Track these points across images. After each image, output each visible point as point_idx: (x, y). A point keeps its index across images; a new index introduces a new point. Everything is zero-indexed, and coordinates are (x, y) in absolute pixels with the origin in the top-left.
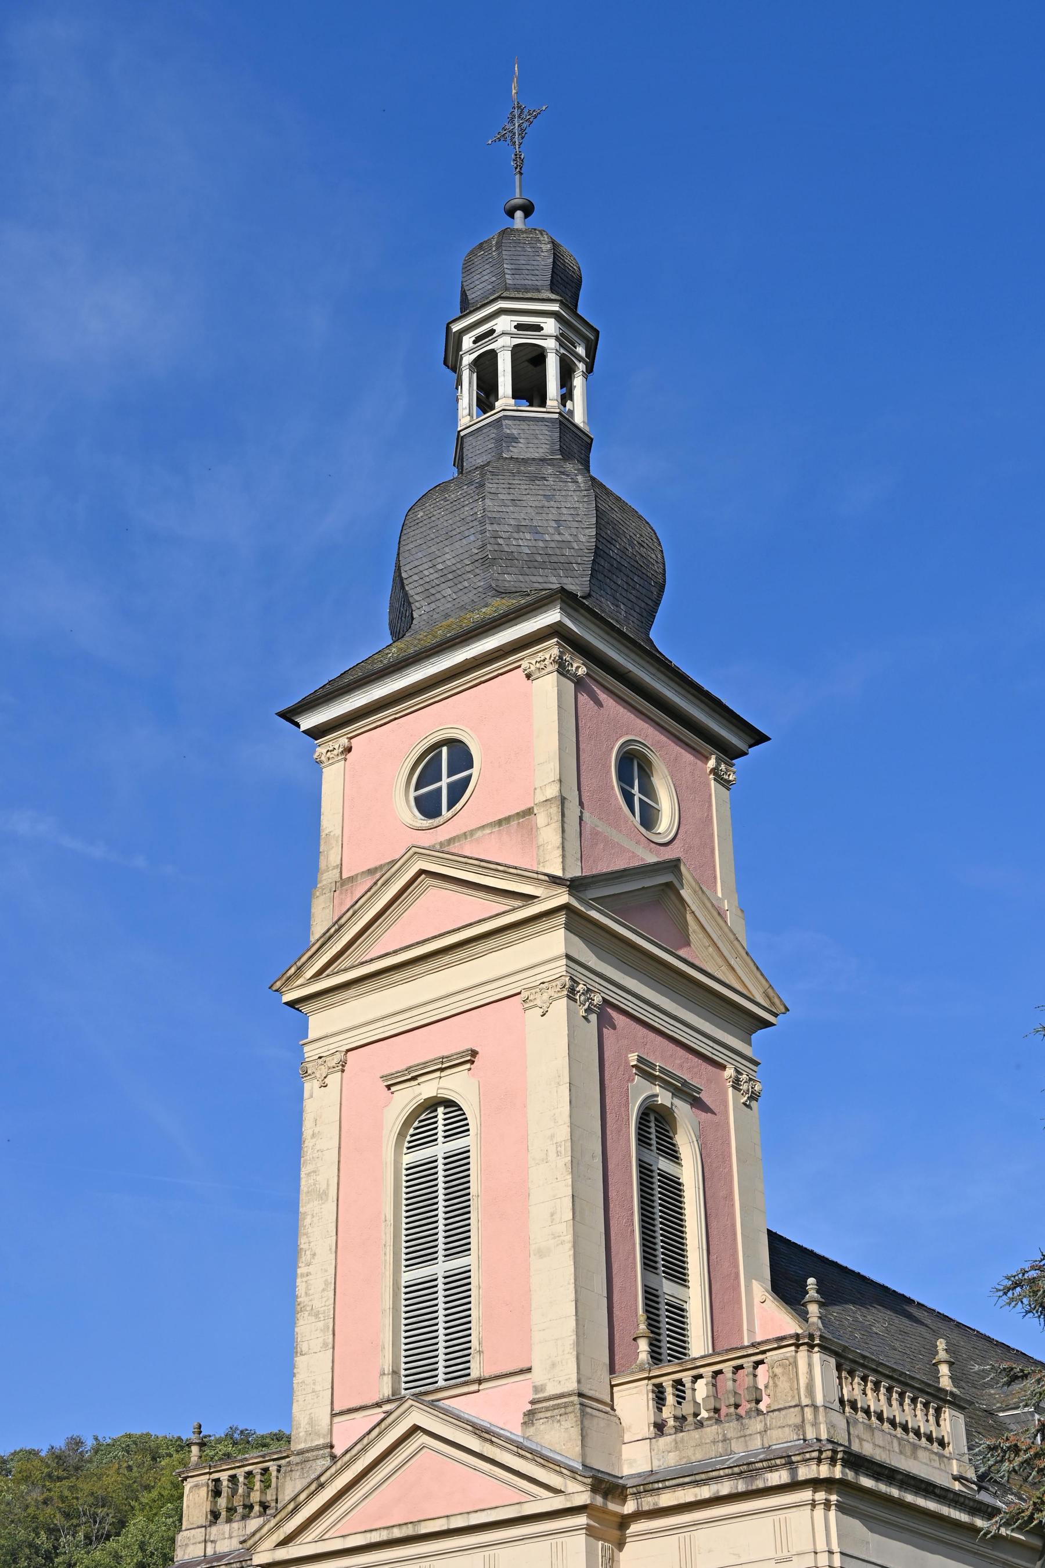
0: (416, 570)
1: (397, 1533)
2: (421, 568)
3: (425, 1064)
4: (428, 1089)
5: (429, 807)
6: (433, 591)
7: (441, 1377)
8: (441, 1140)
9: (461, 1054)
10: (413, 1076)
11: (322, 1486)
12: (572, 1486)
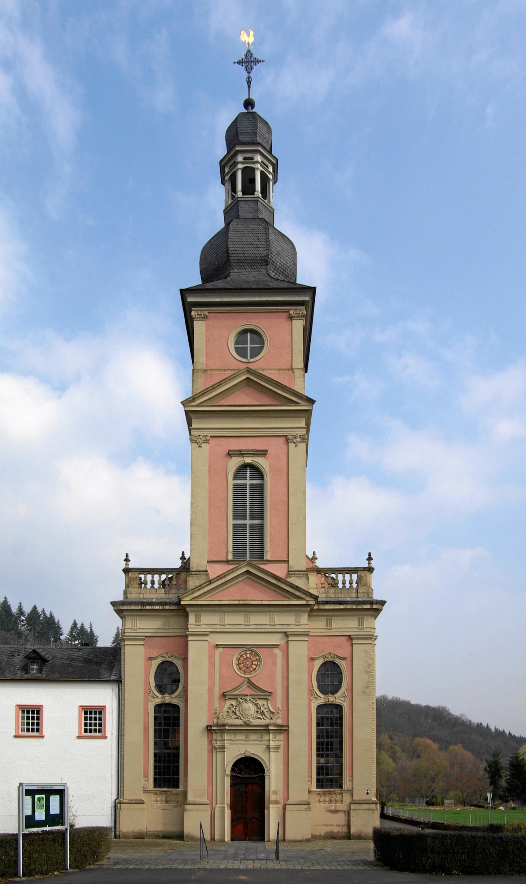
0: (236, 252)
1: (241, 602)
2: (238, 252)
3: (249, 450)
4: (248, 460)
5: (241, 352)
6: (241, 264)
7: (248, 557)
8: (248, 479)
9: (262, 451)
10: (241, 453)
11: (211, 583)
12: (308, 599)
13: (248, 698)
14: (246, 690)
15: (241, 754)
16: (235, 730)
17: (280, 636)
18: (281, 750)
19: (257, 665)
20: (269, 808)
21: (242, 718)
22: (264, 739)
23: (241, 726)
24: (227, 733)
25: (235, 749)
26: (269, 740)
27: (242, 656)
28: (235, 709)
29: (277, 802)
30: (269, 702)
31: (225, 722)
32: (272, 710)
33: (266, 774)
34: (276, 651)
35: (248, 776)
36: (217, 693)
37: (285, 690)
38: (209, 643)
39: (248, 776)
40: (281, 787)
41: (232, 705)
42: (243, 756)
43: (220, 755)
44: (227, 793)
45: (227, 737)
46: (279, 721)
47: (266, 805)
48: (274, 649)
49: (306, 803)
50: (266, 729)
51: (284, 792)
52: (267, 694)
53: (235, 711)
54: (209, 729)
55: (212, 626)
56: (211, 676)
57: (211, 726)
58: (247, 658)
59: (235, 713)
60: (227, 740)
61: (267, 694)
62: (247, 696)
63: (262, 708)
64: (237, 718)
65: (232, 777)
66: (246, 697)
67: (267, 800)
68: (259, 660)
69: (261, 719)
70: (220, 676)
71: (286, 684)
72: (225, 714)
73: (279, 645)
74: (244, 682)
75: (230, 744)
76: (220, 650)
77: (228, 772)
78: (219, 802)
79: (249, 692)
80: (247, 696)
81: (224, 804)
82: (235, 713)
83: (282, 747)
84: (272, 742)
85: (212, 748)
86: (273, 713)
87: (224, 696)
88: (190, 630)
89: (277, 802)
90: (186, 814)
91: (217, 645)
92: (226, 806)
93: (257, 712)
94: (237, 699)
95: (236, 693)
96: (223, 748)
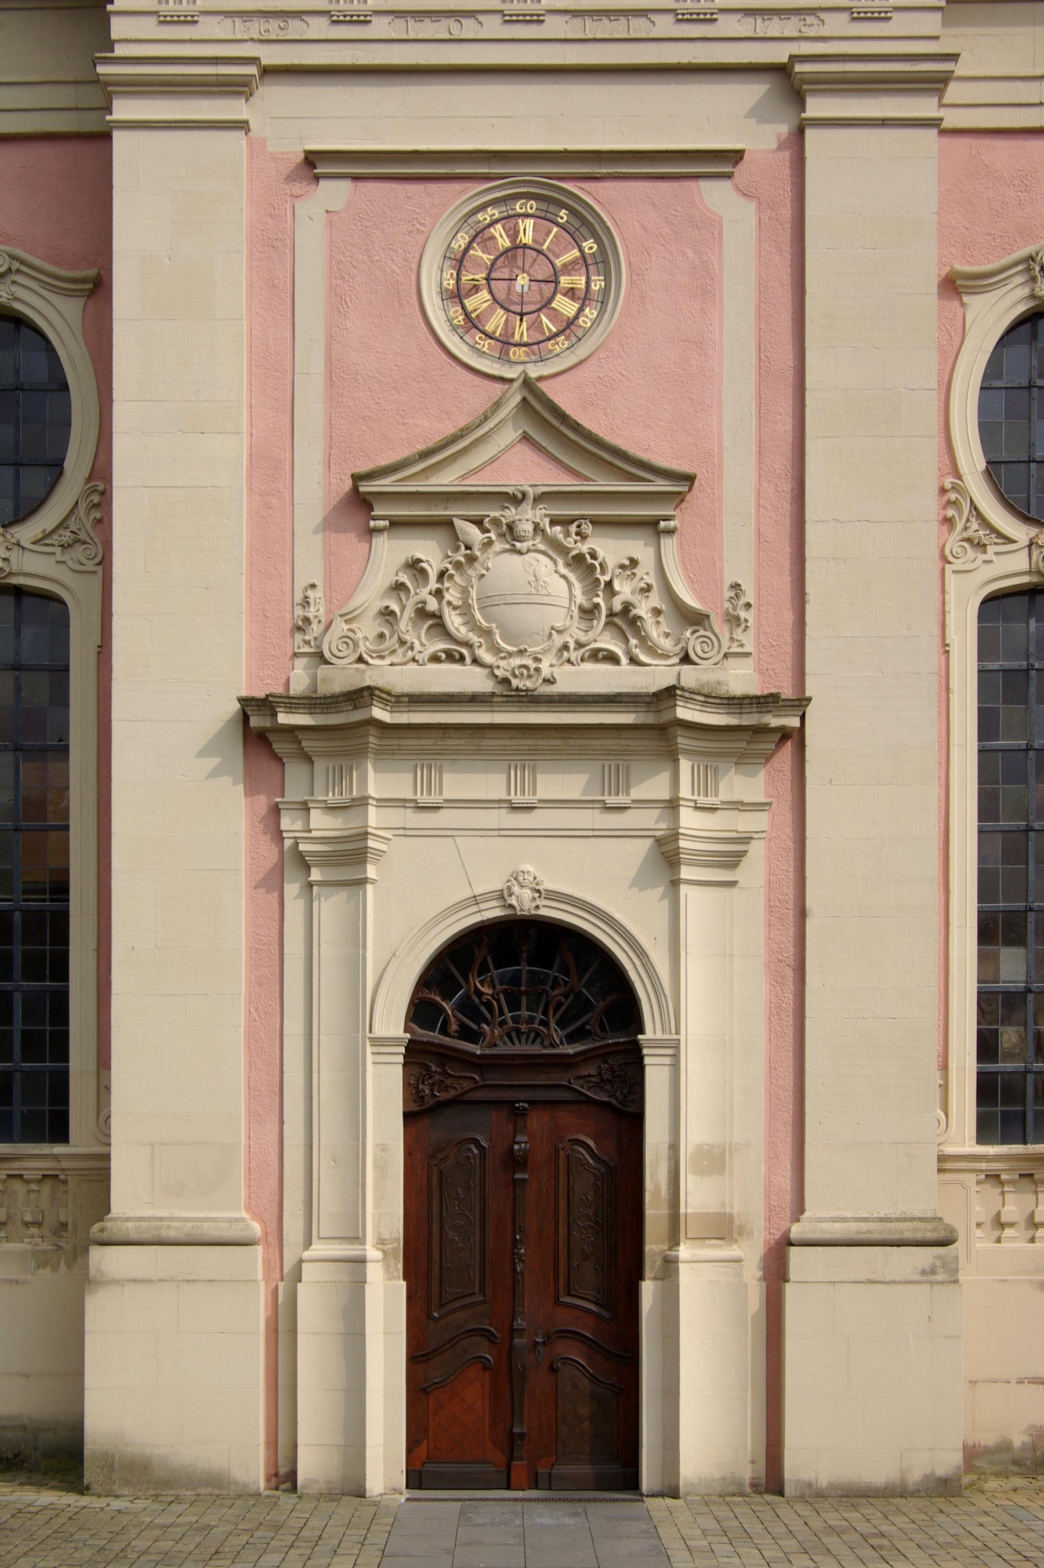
13: (527, 517)
14: (510, 462)
15: (475, 900)
16: (437, 735)
17: (753, 92)
18: (754, 871)
19: (584, 298)
20: (670, 1265)
21: (487, 657)
22: (636, 793)
23: (474, 700)
24: (384, 754)
25: (443, 857)
26: (673, 805)
27: (480, 236)
28: (438, 594)
29: (723, 1228)
30: (668, 544)
31: (370, 679)
32: (690, 600)
33: (651, 1031)
34: (716, 196)
35: (530, 1046)
36: (315, 489)
37: (781, 463)
38: (256, 148)
39: (530, 1046)
40: (752, 1128)
41: (415, 566)
42: (493, 912)
43: (330, 907)
44: (381, 1168)
45: (378, 781)
46: (741, 679)
47: (653, 1246)
48: (705, 186)
49: (926, 1232)
50: (652, 729)
51: (771, 1158)
52: (660, 485)
53: (432, 605)
54: (261, 735)
55: (273, 28)
56: (273, 370)
57: (267, 705)
58: (517, 247)
59: (438, 624)
60: (384, 803)
61: (660, 485)
62: (517, 500)
63: (625, 589)
64: (451, 657)
65: (417, 1056)
66: (511, 513)
67: (654, 1211)
68: (603, 261)
69: (612, 658)
70: (335, 373)
71: (785, 425)
72: (367, 629)
73: (735, 156)
74: (497, 405)
75: (405, 832)
76: (334, 193)
77: (391, 1019)
78: (326, 1221)
79: (528, 471)
80: (517, 500)
81: (358, 1239)
82: (438, 624)
83: (757, 850)
84: (689, 820)
85: (289, 865)
86: (695, 619)
87: (360, 505)
88: (120, 51)
89: (723, 1228)
90: (99, 1311)
91: (312, 160)
92: (372, 1253)
93: (589, 613)
94: (447, 524)
95: (446, 480)
96: (351, 855)
